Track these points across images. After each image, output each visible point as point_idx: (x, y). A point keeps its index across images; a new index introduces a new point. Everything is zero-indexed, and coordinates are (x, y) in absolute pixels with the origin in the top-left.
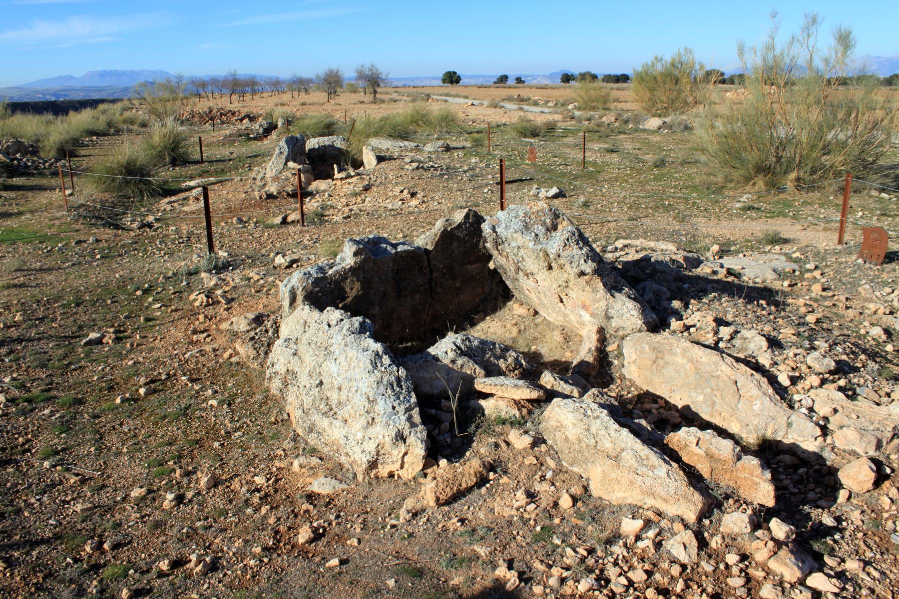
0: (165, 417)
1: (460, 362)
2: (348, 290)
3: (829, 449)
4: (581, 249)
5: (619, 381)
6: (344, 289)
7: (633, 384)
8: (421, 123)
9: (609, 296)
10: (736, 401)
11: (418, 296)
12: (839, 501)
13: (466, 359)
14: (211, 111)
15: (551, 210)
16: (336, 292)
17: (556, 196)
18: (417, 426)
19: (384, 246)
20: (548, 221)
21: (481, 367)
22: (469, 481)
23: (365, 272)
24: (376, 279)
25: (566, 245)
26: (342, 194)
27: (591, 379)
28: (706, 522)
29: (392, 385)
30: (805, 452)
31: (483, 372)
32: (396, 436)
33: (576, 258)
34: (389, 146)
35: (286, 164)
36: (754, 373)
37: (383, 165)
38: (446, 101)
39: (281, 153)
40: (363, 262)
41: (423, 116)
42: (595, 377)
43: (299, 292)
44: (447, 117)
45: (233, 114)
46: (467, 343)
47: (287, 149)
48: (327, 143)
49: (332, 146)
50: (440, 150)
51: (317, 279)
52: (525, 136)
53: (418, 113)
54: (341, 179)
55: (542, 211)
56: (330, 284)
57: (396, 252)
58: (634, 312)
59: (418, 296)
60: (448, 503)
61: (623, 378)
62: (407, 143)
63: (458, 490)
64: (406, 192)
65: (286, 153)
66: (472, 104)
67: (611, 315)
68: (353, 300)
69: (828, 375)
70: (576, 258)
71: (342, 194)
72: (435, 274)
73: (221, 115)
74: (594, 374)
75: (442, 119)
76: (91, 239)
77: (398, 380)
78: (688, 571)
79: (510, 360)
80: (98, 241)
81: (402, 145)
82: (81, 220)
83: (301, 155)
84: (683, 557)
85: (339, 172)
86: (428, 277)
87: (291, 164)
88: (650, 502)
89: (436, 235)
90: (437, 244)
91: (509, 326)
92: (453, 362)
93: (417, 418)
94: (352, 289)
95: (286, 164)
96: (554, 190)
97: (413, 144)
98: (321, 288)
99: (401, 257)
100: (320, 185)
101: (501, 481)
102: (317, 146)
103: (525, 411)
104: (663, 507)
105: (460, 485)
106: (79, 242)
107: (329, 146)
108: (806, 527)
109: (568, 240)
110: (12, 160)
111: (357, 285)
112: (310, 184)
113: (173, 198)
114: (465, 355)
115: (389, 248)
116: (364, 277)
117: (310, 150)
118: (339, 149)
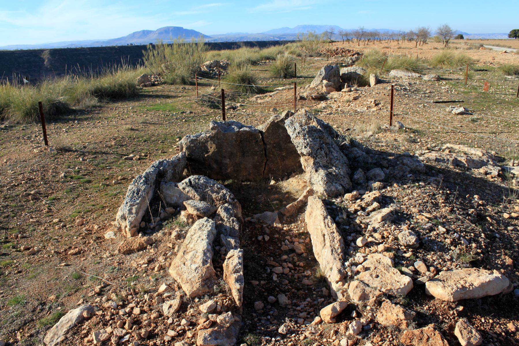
0: (107, 195)
1: (187, 189)
2: (209, 148)
3: (341, 291)
4: (305, 139)
5: (300, 222)
6: (207, 147)
7: (306, 225)
8: (446, 63)
9: (314, 171)
10: (322, 248)
11: (256, 157)
12: (313, 323)
13: (190, 188)
14: (337, 50)
15: (306, 115)
16: (203, 148)
17: (461, 113)
18: (133, 214)
19: (233, 126)
20: (304, 121)
21: (199, 195)
22: (135, 246)
23: (218, 139)
24: (225, 144)
25: (297, 136)
26: (341, 101)
27: (285, 218)
28: (197, 300)
29: (134, 192)
30: (332, 289)
31: (199, 197)
32: (122, 216)
33: (301, 144)
34: (402, 76)
35: (322, 81)
36: (335, 231)
37: (378, 86)
38: (491, 49)
39: (321, 75)
40: (217, 134)
41: (448, 58)
42: (288, 217)
43: (184, 146)
44: (462, 60)
45: (349, 51)
46: (197, 181)
47: (324, 73)
48: (352, 71)
49: (355, 73)
50: (433, 79)
51: (192, 140)
52: (509, 74)
53: (445, 56)
54: (345, 92)
55: (301, 115)
56: (199, 143)
57: (239, 131)
58: (321, 183)
59: (256, 157)
60: (124, 253)
61: (303, 221)
62: (414, 74)
63: (130, 249)
64: (373, 103)
65: (323, 75)
66: (506, 52)
67: (313, 183)
68: (212, 153)
69: (403, 247)
70: (301, 144)
71: (341, 101)
72: (268, 146)
73: (343, 52)
74: (288, 215)
75: (459, 61)
76: (188, 112)
77: (138, 191)
78: (160, 319)
79: (221, 194)
80: (191, 113)
81: (410, 75)
82: (200, 103)
83: (334, 76)
84: (166, 312)
85: (347, 88)
86: (263, 147)
87: (325, 82)
88: (179, 281)
89: (268, 124)
90: (268, 129)
91: (301, 182)
92: (184, 189)
93: (134, 211)
94: (211, 148)
95: (322, 81)
96: (462, 109)
97: (417, 75)
98: (195, 145)
99: (242, 134)
100: (335, 94)
101: (151, 251)
102: (347, 72)
103: (191, 220)
104: (183, 286)
105: (131, 247)
106: (183, 113)
107: (354, 72)
108: (268, 328)
109: (299, 133)
110: (210, 71)
111: (214, 146)
112: (329, 93)
113: (261, 95)
114: (193, 187)
115: (236, 128)
116: (218, 142)
117: (343, 74)
118: (359, 75)
